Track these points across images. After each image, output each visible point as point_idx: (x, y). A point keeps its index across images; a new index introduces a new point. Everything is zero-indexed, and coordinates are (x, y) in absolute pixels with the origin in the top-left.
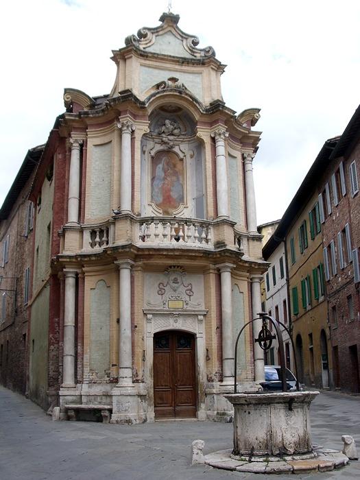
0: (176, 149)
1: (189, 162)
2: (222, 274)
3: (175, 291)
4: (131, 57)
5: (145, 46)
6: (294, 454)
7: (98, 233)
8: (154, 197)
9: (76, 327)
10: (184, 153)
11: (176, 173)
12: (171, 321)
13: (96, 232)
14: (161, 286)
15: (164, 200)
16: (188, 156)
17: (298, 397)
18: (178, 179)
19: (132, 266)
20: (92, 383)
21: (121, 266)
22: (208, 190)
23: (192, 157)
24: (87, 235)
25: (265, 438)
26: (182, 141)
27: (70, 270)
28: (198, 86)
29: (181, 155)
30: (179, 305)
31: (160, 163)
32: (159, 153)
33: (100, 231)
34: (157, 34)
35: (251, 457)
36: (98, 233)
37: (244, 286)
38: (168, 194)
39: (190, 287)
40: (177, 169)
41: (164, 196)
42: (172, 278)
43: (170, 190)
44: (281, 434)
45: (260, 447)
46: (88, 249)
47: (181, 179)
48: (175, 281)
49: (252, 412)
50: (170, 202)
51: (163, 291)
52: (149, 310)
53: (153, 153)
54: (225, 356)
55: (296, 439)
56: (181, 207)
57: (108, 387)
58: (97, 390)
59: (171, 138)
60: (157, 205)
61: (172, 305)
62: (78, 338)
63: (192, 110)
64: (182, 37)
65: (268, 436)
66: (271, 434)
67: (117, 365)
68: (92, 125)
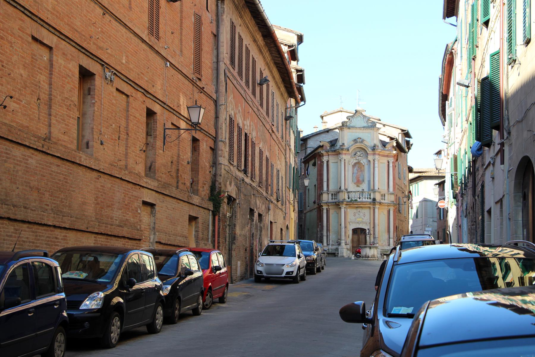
0: (362, 162)
1: (366, 167)
11: (361, 171)
12: (358, 224)
20: (332, 245)
27: (325, 207)
30: (361, 219)
32: (356, 164)
33: (336, 194)
37: (386, 212)
46: (330, 200)
48: (359, 212)
57: (337, 246)
58: (334, 247)
61: (358, 219)
62: (328, 230)
67: (340, 239)
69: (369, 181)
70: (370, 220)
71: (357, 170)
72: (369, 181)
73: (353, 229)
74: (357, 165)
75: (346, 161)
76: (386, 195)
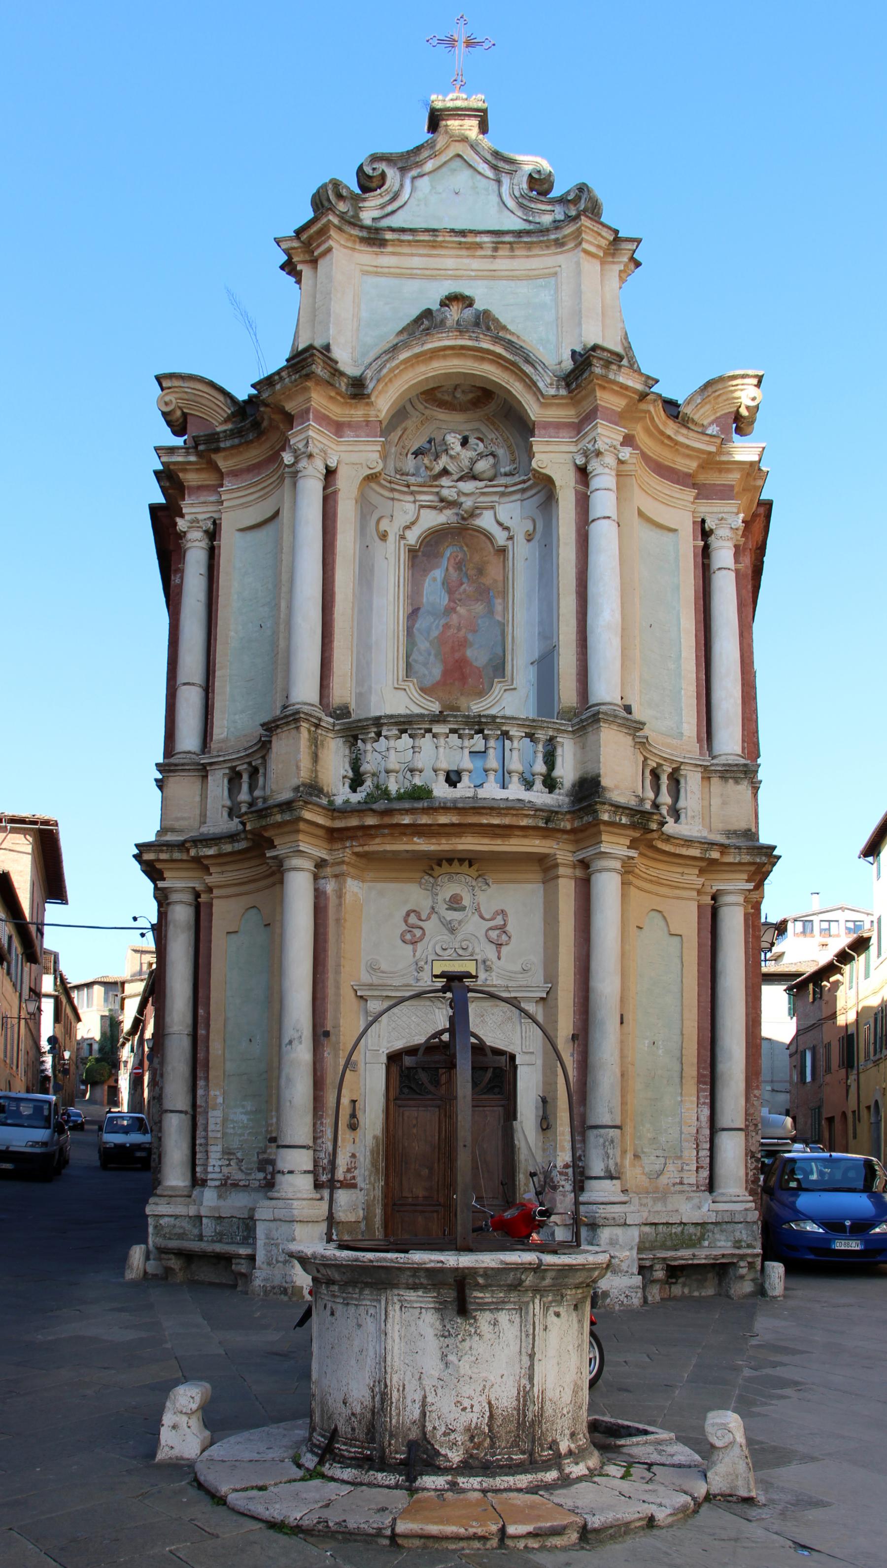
0: (486, 521)
2: (594, 878)
3: (452, 931)
4: (329, 250)
5: (377, 214)
6: (467, 1467)
7: (245, 777)
8: (417, 667)
9: (194, 1036)
10: (507, 529)
11: (484, 594)
13: (239, 775)
14: (413, 919)
15: (446, 673)
16: (520, 538)
17: (487, 1273)
18: (491, 612)
19: (320, 864)
21: (288, 864)
22: (563, 628)
23: (529, 538)
24: (218, 784)
25: (367, 1402)
26: (503, 494)
28: (547, 309)
29: (500, 537)
31: (438, 567)
34: (414, 173)
35: (321, 1462)
36: (245, 777)
37: (686, 917)
38: (457, 656)
39: (499, 921)
40: (487, 581)
41: (444, 662)
42: (448, 889)
43: (464, 644)
44: (418, 1397)
45: (353, 1429)
47: (499, 608)
48: (455, 904)
49: (339, 1309)
50: (463, 679)
51: (418, 933)
52: (371, 986)
53: (413, 537)
54: (186, 1119)
55: (476, 1417)
56: (498, 688)
59: (468, 486)
60: (423, 690)
63: (517, 389)
64: (495, 168)
65: (377, 1398)
66: (382, 1396)
68: (235, 474)
69: (546, 664)
70: (551, 976)
71: (450, 588)
72: (546, 664)
73: (394, 1058)
74: (448, 551)
75: (347, 486)
76: (692, 781)
